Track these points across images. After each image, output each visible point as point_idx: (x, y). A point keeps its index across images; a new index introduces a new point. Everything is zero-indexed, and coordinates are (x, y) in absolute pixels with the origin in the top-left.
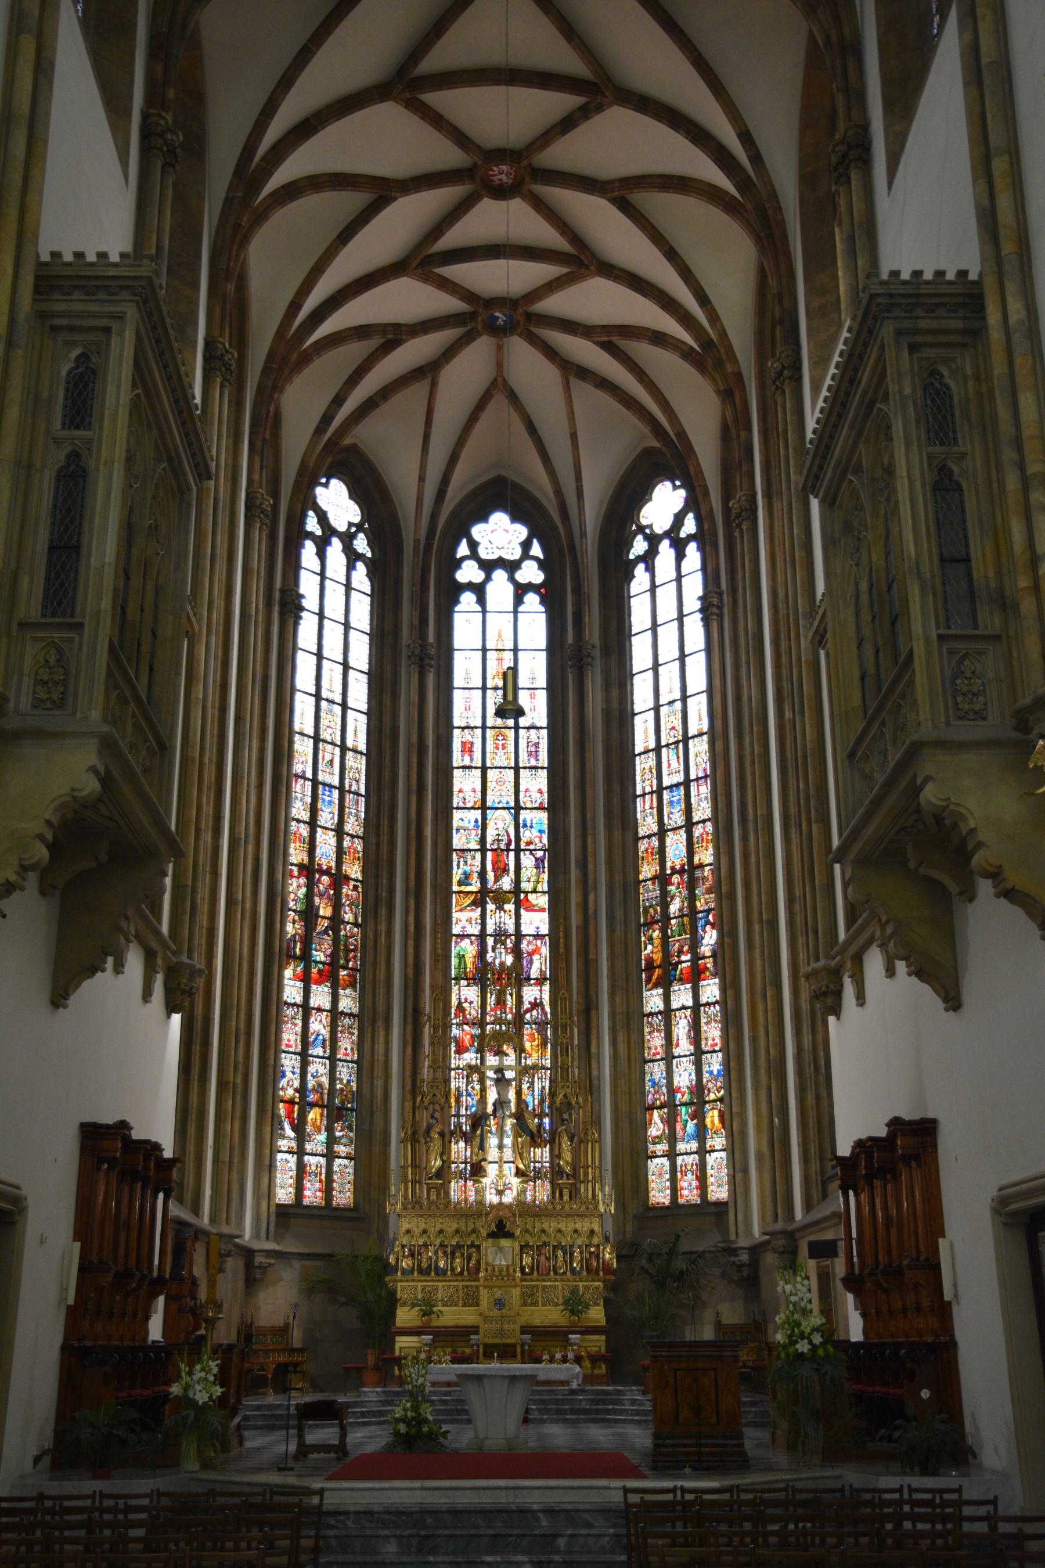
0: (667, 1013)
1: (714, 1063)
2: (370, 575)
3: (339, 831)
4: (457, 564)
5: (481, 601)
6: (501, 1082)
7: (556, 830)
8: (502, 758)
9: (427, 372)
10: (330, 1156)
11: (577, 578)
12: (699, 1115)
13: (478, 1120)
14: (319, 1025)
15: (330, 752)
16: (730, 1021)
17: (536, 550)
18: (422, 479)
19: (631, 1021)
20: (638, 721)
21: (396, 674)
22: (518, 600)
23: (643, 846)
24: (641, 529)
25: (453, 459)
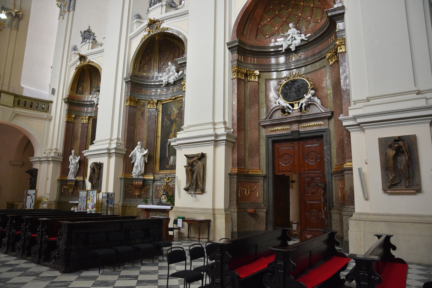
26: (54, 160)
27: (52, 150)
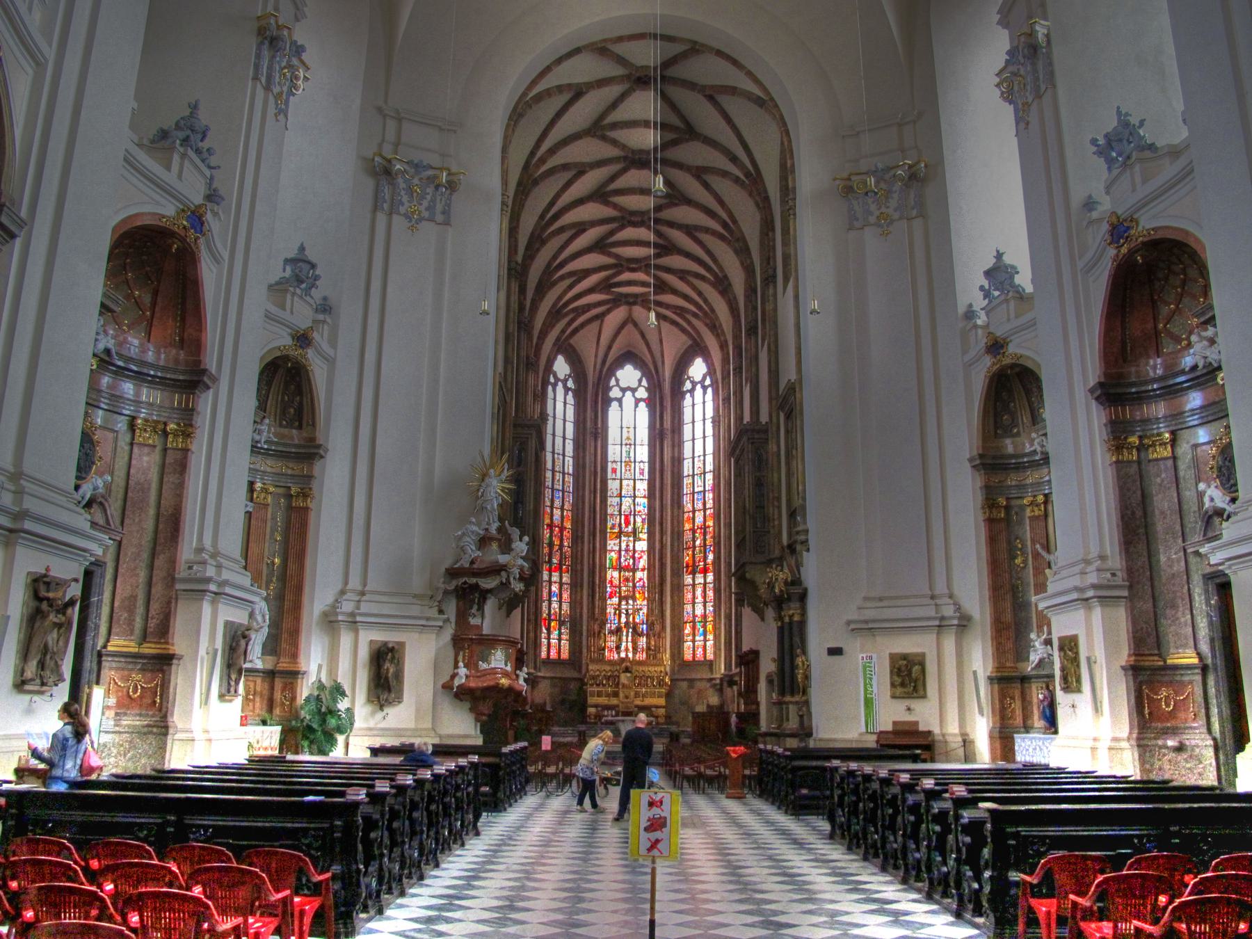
0: (694, 585)
1: (710, 608)
2: (574, 397)
3: (562, 509)
4: (610, 389)
5: (621, 406)
6: (627, 614)
10: (560, 640)
11: (662, 399)
12: (704, 626)
13: (618, 631)
14: (555, 588)
16: (717, 591)
17: (644, 383)
19: (678, 588)
21: (584, 441)
22: (636, 406)
23: (686, 515)
24: (689, 378)
25: (610, 348)
27: (1087, 562)
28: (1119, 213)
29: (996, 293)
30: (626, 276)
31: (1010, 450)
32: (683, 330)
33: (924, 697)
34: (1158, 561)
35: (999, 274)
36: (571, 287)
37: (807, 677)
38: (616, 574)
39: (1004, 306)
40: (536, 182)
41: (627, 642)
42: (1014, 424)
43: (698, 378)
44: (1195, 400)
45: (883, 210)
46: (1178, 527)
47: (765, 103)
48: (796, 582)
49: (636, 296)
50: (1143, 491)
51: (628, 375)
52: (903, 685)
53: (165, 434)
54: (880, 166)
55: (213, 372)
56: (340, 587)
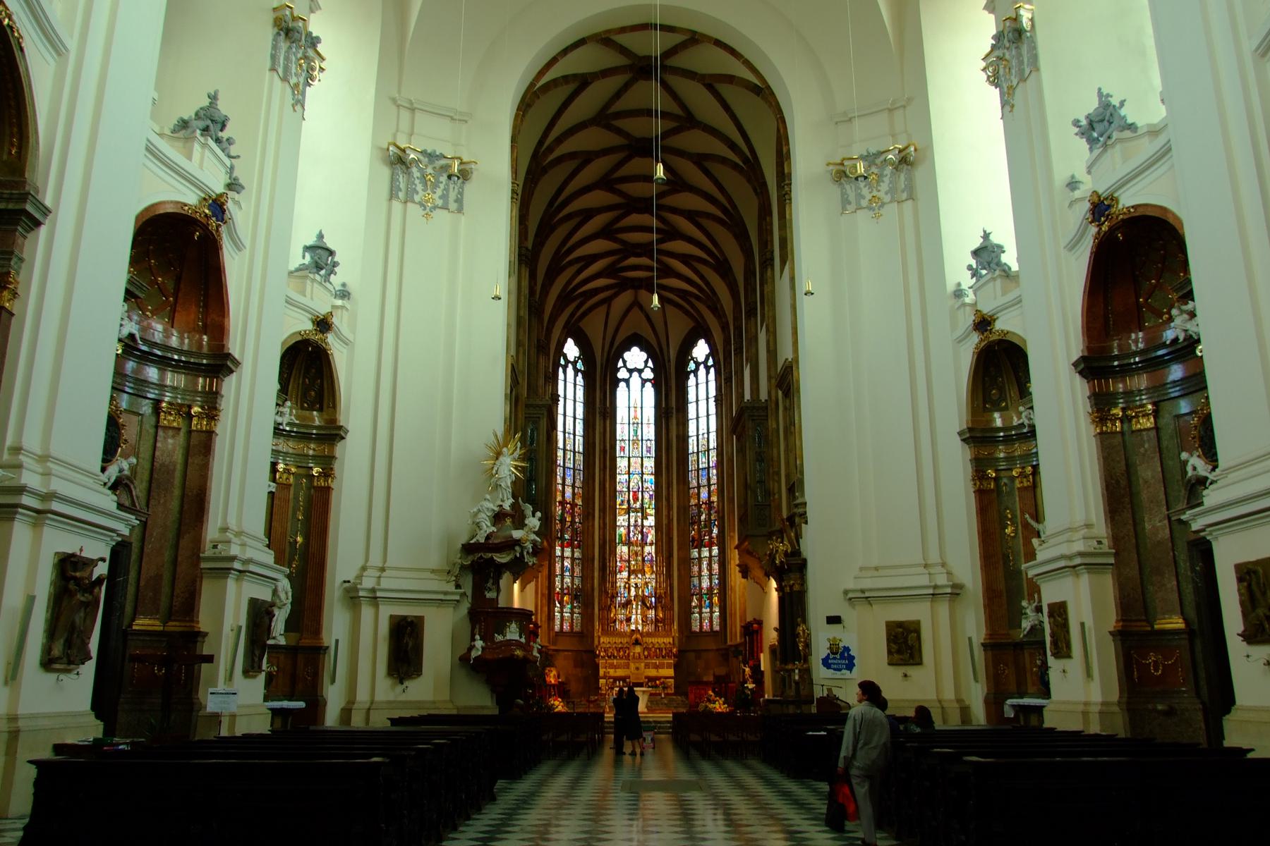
0: (700, 559)
3: (573, 486)
4: (618, 370)
5: (628, 386)
7: (658, 484)
8: (637, 453)
9: (608, 301)
10: (572, 613)
13: (628, 603)
14: (567, 563)
15: (570, 455)
17: (650, 364)
18: (604, 339)
19: (686, 562)
20: (690, 440)
22: (643, 386)
26: (1089, 564)
28: (1100, 192)
29: (984, 272)
30: (632, 261)
31: (999, 423)
32: (687, 313)
33: (920, 663)
34: (1144, 528)
35: (986, 254)
36: (579, 272)
37: (808, 645)
38: (625, 549)
39: (991, 284)
40: (545, 171)
41: (636, 616)
42: (1002, 397)
43: (701, 359)
44: (1176, 372)
45: (875, 193)
46: (1162, 496)
47: (763, 92)
48: (796, 553)
49: (640, 279)
50: (1127, 460)
51: (635, 357)
52: (899, 652)
53: (190, 417)
54: (873, 150)
55: (237, 356)
56: (361, 563)
